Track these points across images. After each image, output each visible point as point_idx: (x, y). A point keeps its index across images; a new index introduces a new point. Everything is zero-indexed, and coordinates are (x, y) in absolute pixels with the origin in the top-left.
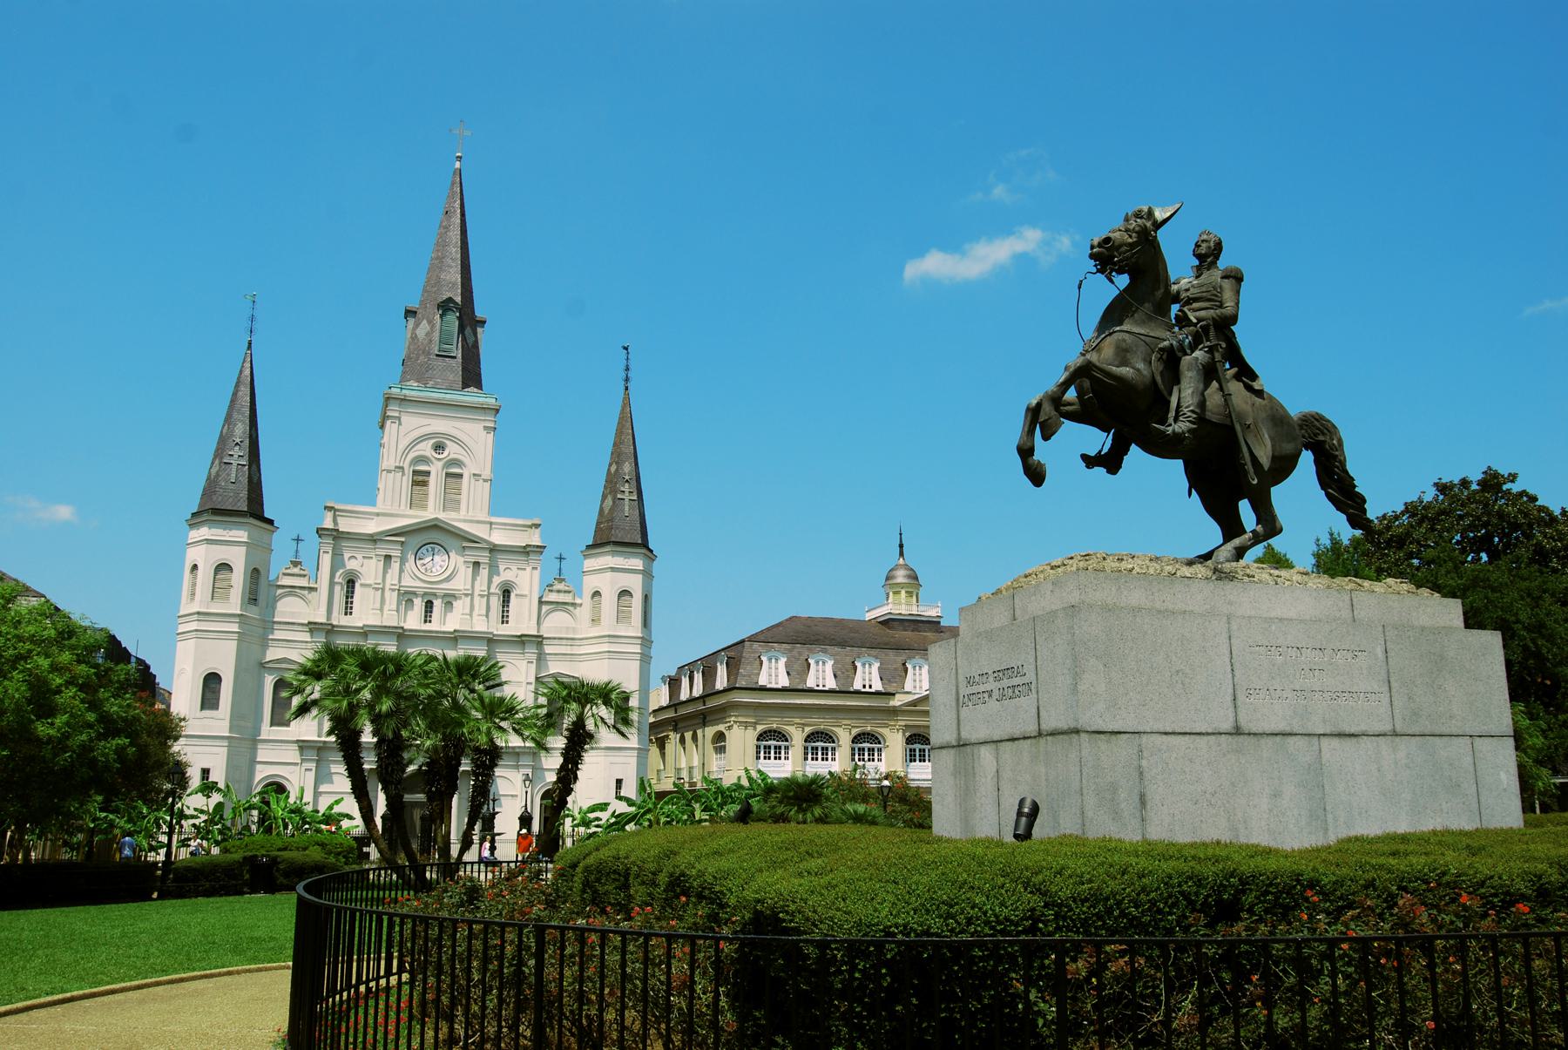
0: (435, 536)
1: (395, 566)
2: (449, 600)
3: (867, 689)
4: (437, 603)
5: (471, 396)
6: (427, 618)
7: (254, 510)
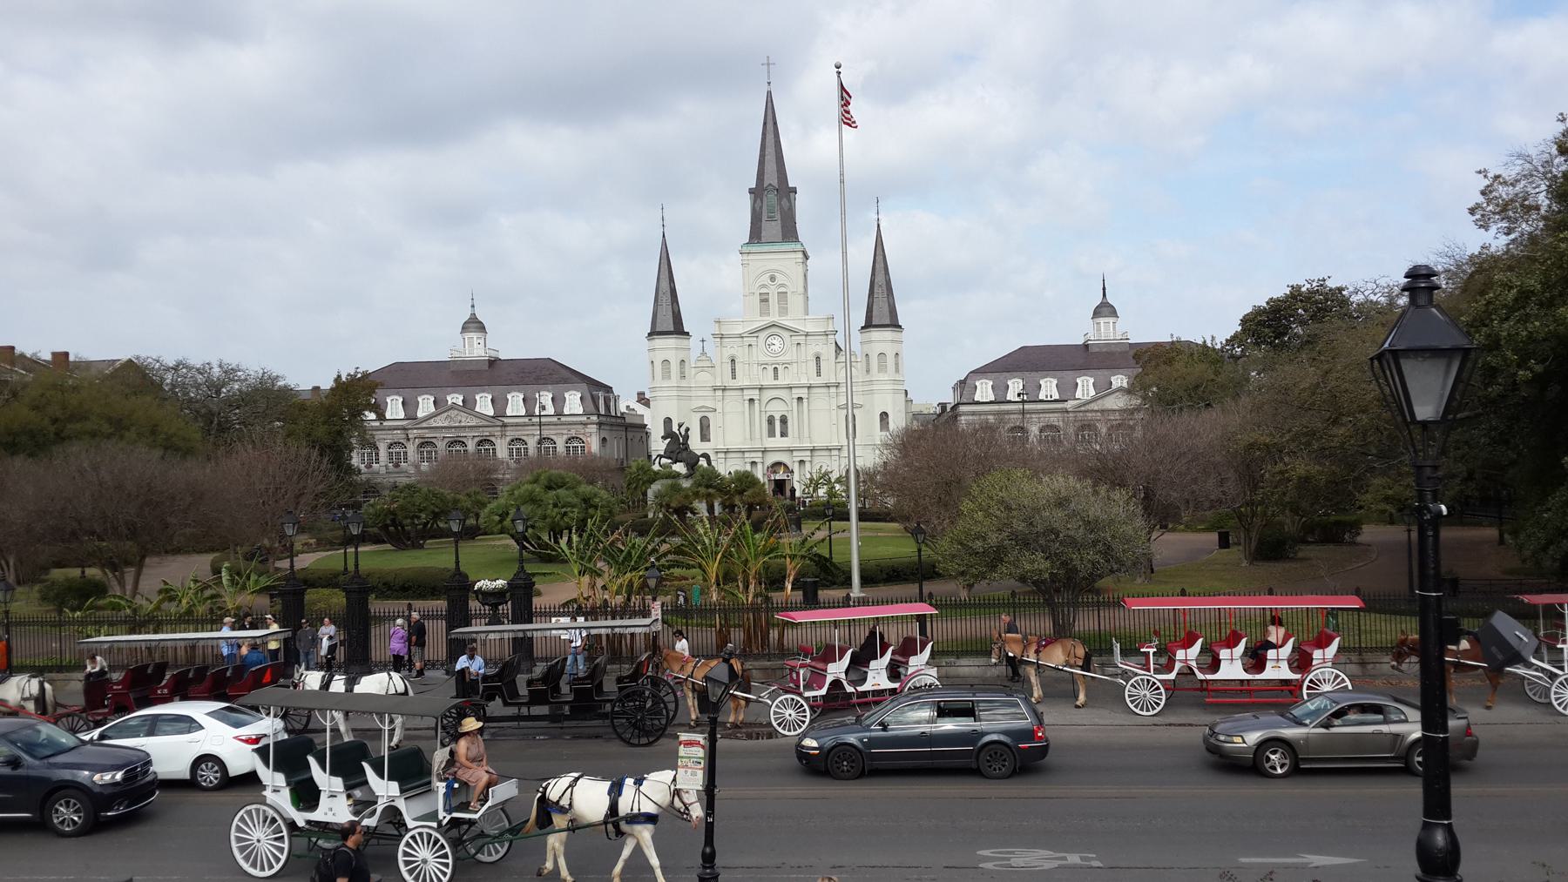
0: (774, 330)
1: (754, 349)
2: (786, 365)
3: (1049, 399)
4: (780, 368)
5: (792, 246)
6: (776, 377)
7: (679, 330)
